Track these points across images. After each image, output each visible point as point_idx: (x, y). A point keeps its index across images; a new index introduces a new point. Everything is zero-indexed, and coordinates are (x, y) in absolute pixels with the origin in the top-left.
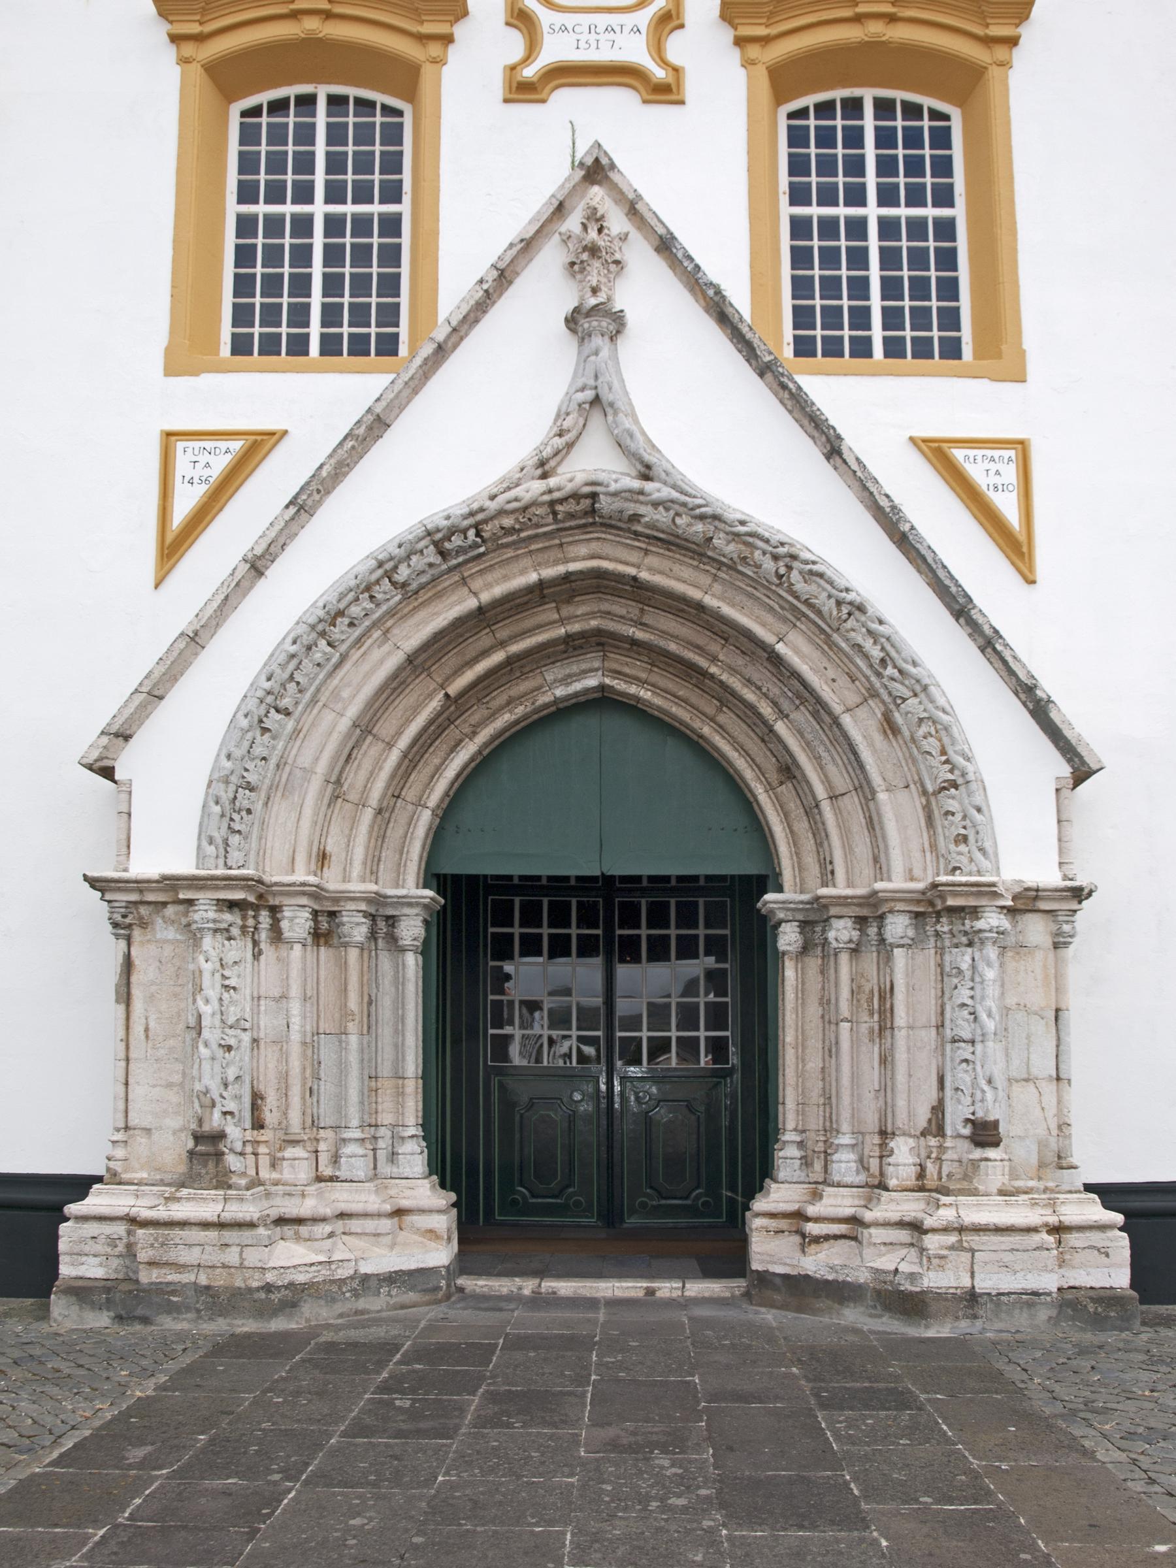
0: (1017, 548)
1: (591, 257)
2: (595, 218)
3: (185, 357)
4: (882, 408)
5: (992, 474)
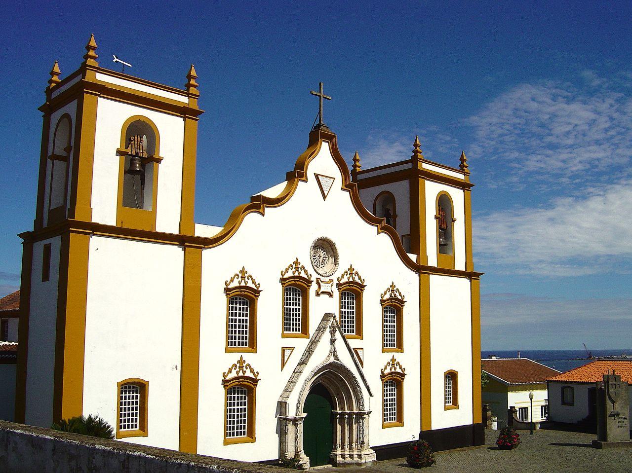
0: (362, 363)
3: (284, 336)
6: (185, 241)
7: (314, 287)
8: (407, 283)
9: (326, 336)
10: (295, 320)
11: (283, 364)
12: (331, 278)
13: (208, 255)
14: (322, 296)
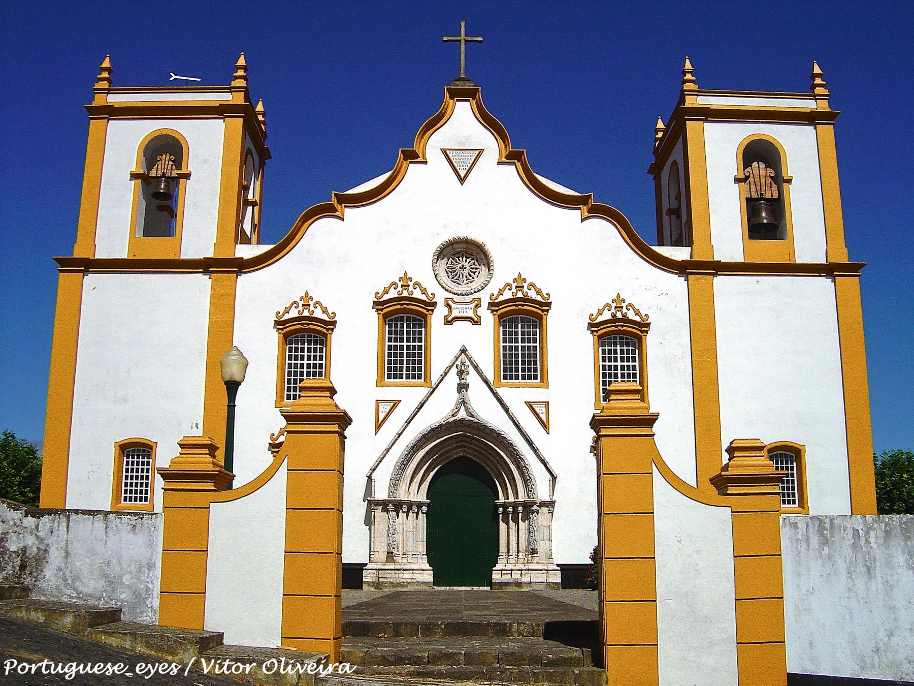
0: (545, 426)
2: (463, 364)
3: (380, 384)
7: (440, 312)
8: (657, 295)
9: (453, 379)
11: (379, 426)
12: (476, 296)
13: (246, 282)
14: (456, 323)
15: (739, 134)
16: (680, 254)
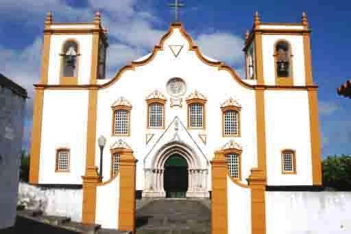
0: (205, 143)
1: (177, 124)
4: (195, 132)
5: (203, 138)
6: (92, 87)
8: (246, 99)
9: (173, 126)
10: (155, 121)
11: (147, 143)
13: (100, 92)
15: (276, 38)
16: (254, 82)
